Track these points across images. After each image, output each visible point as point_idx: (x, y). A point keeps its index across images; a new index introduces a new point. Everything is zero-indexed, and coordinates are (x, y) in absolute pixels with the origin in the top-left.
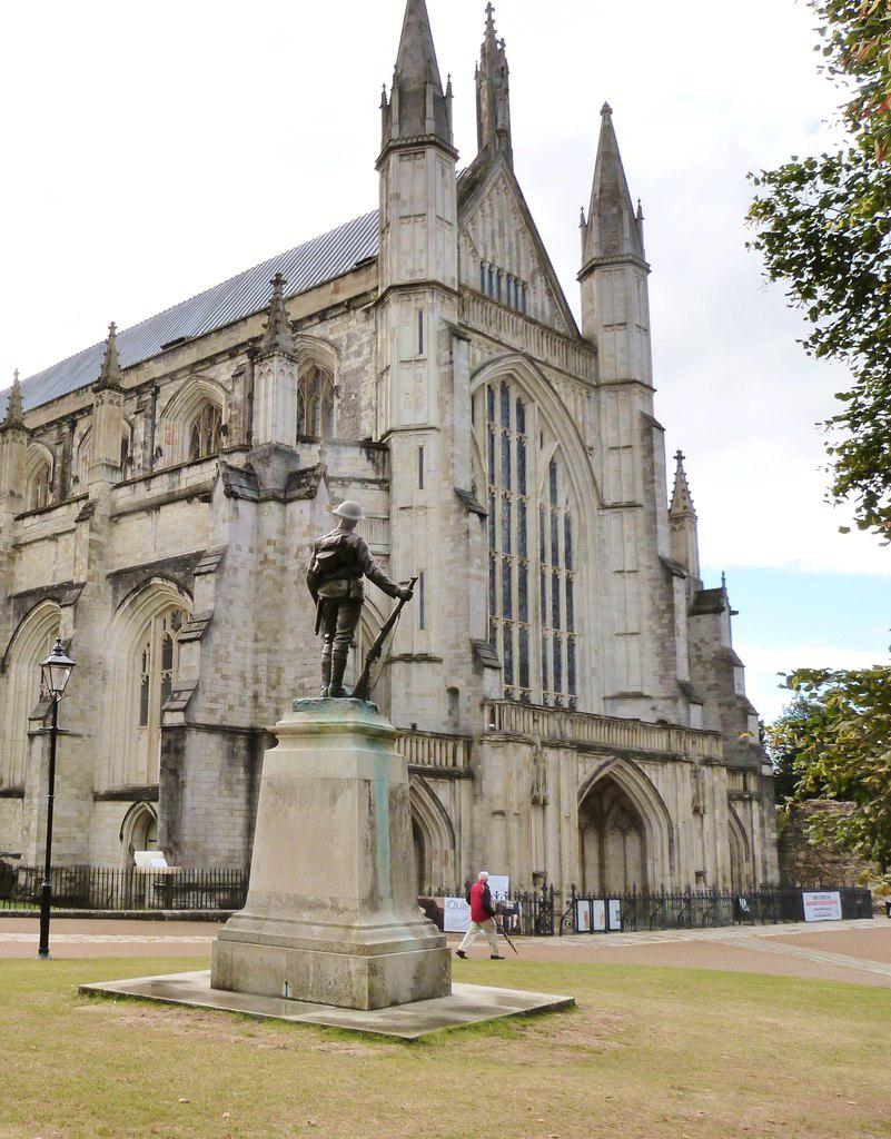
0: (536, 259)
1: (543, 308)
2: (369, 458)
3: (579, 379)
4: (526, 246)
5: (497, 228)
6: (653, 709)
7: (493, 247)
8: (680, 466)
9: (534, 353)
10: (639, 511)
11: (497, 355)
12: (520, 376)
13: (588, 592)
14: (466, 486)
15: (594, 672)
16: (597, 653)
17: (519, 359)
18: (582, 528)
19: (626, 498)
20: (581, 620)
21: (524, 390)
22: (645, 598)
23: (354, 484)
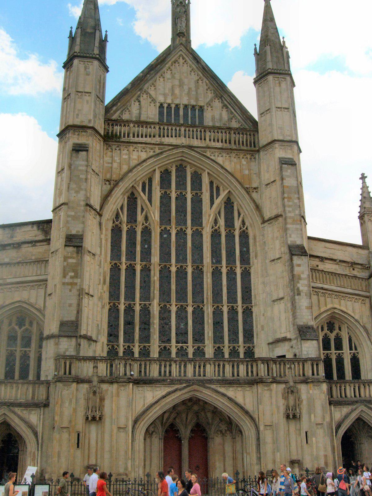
0: (213, 91)
1: (221, 115)
2: (39, 229)
3: (240, 150)
4: (203, 85)
5: (177, 83)
6: (292, 347)
7: (173, 94)
8: (364, 182)
9: (196, 143)
10: (280, 219)
11: (158, 151)
12: (186, 158)
13: (258, 278)
14: (78, 232)
15: (263, 327)
16: (264, 315)
17: (180, 150)
18: (255, 239)
19: (274, 213)
20: (255, 296)
21: (195, 166)
22: (285, 274)
23: (26, 245)
